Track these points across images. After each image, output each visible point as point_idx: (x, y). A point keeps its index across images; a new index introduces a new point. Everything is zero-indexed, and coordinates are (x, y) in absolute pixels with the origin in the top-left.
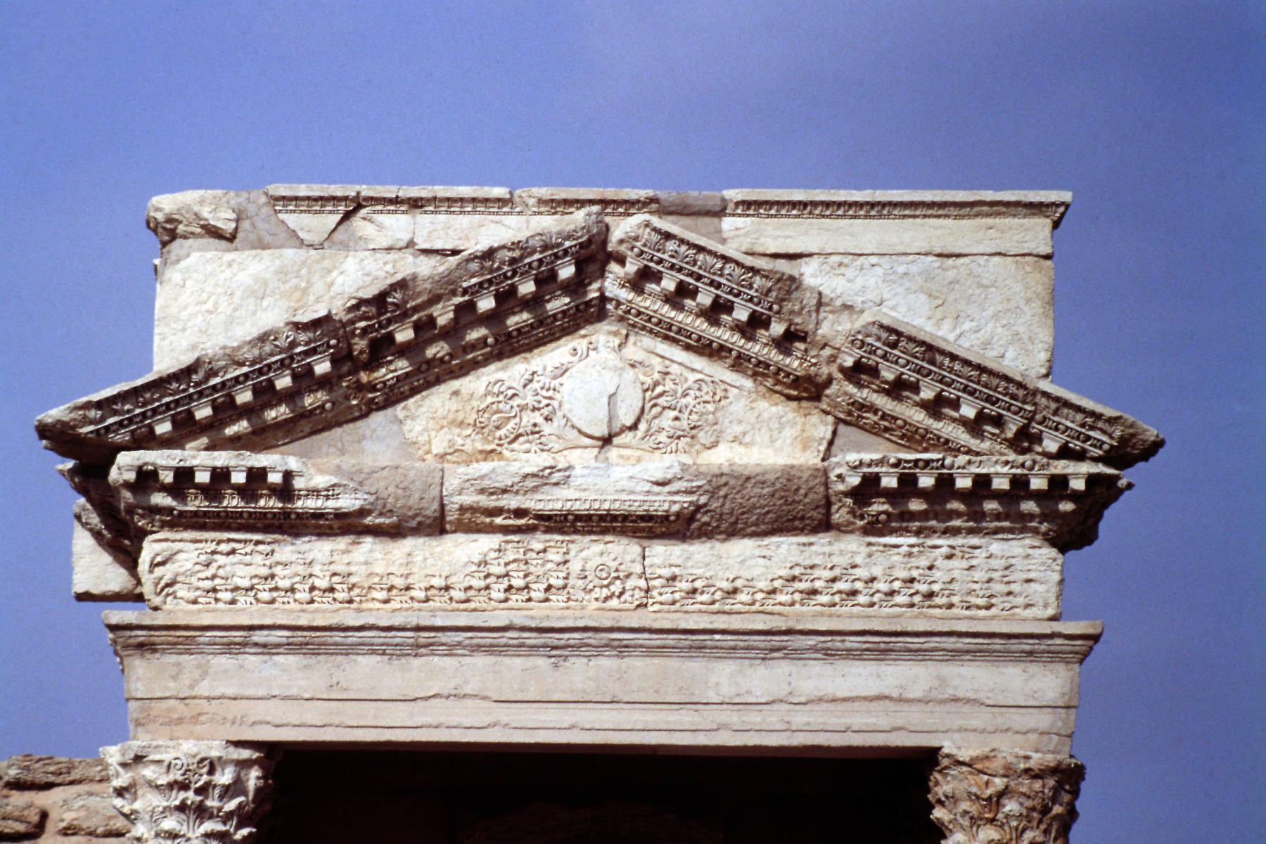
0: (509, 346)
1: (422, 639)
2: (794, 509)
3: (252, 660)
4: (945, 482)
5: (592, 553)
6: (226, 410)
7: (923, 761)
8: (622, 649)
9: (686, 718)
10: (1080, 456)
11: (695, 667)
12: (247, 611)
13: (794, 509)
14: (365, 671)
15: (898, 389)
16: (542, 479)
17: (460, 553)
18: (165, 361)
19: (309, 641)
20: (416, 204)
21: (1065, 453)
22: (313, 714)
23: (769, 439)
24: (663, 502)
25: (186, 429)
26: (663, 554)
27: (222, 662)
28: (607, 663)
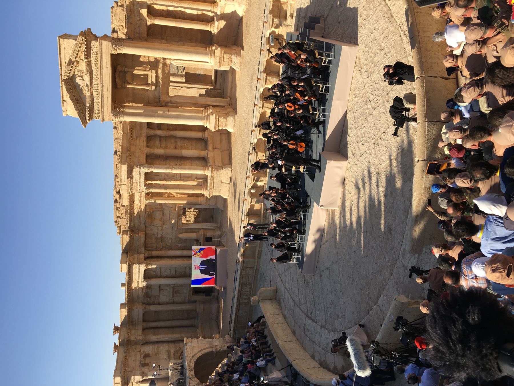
1: (102, 97)
2: (89, 64)
6: (83, 113)
7: (112, 55)
11: (104, 74)
12: (100, 111)
13: (89, 64)
14: (105, 102)
15: (77, 54)
18: (78, 117)
19: (103, 107)
20: (63, 95)
22: (109, 107)
23: (83, 66)
24: (89, 76)
25: (85, 116)
28: (104, 82)
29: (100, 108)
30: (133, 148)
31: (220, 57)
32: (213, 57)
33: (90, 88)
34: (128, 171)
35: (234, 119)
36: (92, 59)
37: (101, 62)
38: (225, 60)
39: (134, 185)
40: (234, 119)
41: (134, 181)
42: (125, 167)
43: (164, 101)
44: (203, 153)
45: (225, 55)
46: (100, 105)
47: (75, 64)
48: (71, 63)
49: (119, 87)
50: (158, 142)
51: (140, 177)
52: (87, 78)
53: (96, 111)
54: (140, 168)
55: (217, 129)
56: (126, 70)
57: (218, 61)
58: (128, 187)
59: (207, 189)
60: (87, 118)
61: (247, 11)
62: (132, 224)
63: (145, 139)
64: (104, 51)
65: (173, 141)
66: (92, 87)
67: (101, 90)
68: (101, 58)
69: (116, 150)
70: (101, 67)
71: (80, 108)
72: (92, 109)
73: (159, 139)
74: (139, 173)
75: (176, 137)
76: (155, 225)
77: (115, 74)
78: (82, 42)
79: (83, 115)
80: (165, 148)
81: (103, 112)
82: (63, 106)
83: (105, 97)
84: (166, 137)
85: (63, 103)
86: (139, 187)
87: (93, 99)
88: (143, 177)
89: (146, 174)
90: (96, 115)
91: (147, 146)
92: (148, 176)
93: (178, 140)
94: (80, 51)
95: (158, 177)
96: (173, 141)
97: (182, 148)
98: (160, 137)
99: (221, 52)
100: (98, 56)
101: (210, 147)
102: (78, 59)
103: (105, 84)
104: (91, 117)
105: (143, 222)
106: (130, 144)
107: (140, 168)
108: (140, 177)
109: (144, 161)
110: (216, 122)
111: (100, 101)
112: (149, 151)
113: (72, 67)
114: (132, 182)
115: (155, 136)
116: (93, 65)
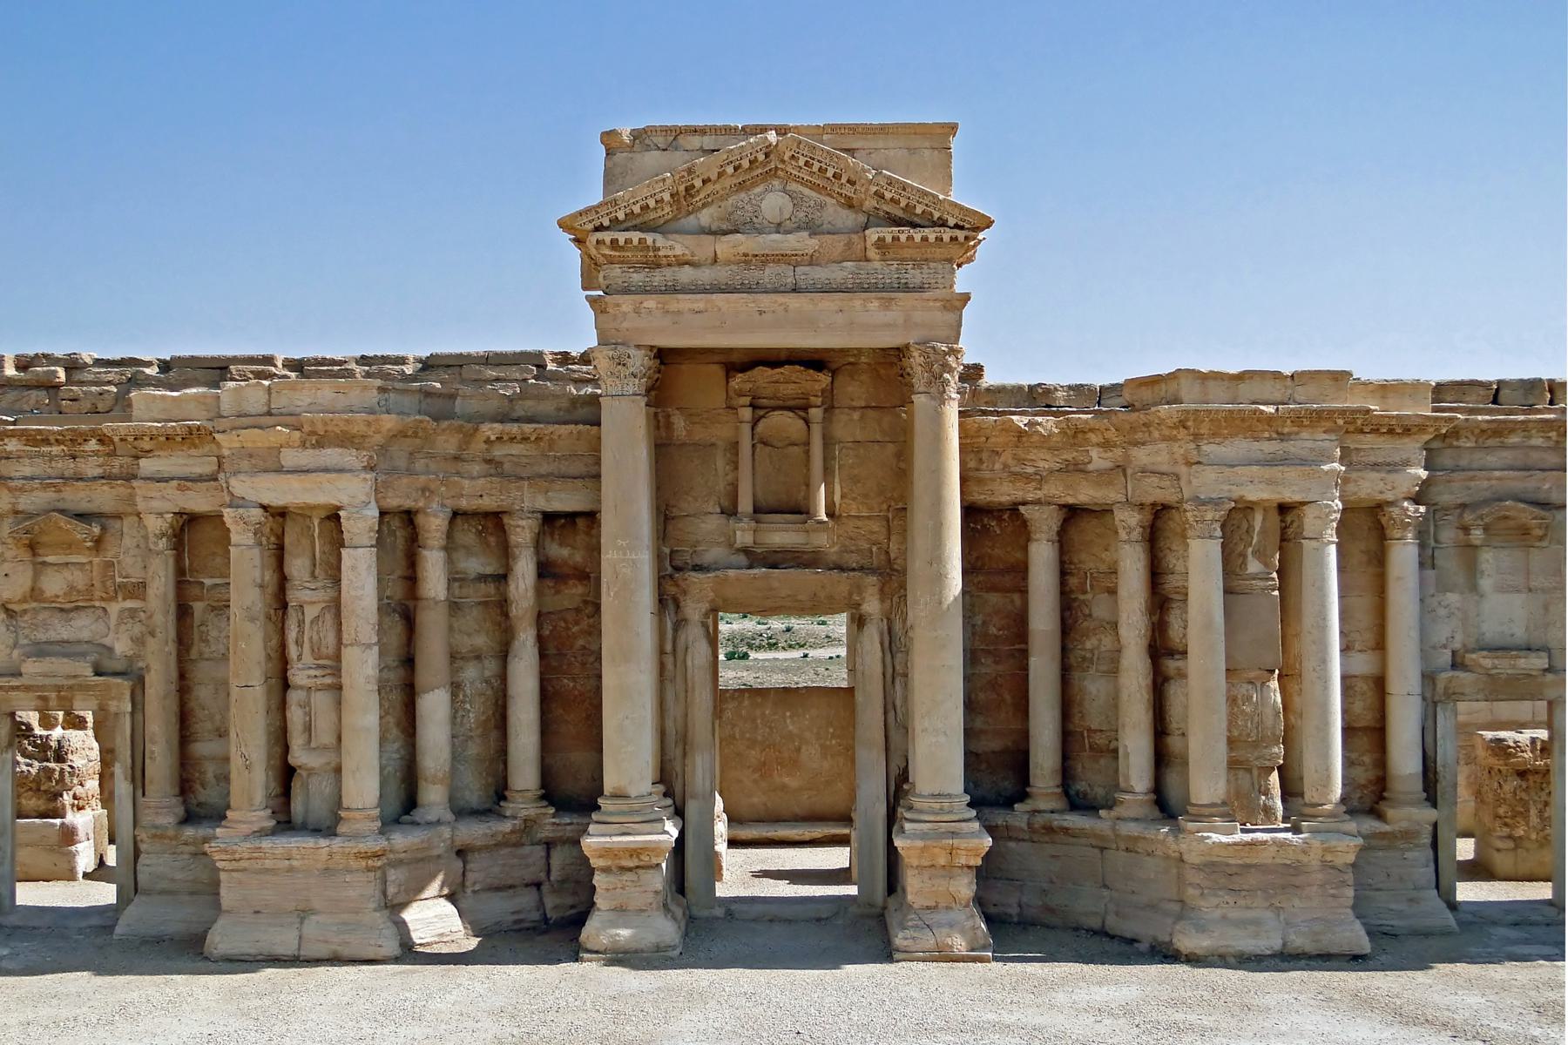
0: (741, 186)
4: (910, 238)
10: (962, 228)
21: (957, 226)
43: (685, 593)
44: (433, 796)
49: (738, 381)
50: (475, 565)
55: (594, 862)
56: (816, 414)
63: (488, 503)
65: (481, 641)
71: (652, 203)
73: (489, 570)
75: (504, 655)
77: (790, 362)
79: (621, 216)
80: (454, 607)
84: (502, 605)
91: (456, 514)
93: (491, 667)
96: (481, 641)
97: (456, 687)
98: (502, 578)
109: (393, 502)
112: (434, 525)
115: (505, 552)
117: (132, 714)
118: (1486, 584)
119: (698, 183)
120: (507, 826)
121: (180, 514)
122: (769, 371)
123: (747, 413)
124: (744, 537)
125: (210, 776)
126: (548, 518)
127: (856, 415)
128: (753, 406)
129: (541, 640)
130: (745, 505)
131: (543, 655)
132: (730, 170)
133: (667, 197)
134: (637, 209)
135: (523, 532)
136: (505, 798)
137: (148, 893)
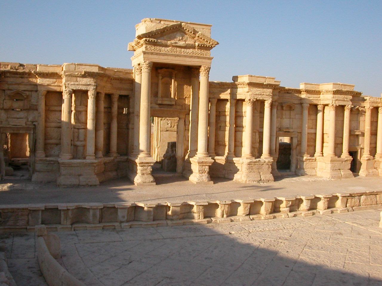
0: (173, 32)
3: (153, 55)
5: (178, 49)
8: (180, 57)
9: (184, 62)
12: (153, 51)
13: (193, 47)
14: (161, 57)
15: (201, 38)
16: (176, 43)
17: (169, 48)
19: (157, 54)
23: (190, 42)
24: (183, 45)
25: (149, 37)
26: (183, 50)
27: (151, 55)
28: (179, 57)
29: (156, 51)
30: (105, 79)
31: (206, 163)
32: (205, 156)
33: (174, 45)
34: (90, 72)
35: (152, 182)
36: (196, 50)
37: (195, 57)
38: (204, 167)
39: (75, 79)
40: (152, 182)
41: (78, 79)
42: (95, 70)
45: (207, 167)
46: (158, 52)
47: (193, 35)
48: (195, 32)
49: (159, 71)
51: (84, 85)
52: (182, 43)
53: (153, 48)
54: (94, 86)
57: (203, 160)
58: (72, 72)
59: (70, 159)
60: (148, 39)
61: (237, 183)
62: (8, 75)
63: (111, 92)
64: (204, 60)
66: (173, 46)
67: (169, 55)
68: (199, 57)
69: (24, 66)
70: (192, 57)
72: (155, 44)
74: (88, 85)
76: (5, 101)
78: (211, 44)
79: (150, 35)
81: (152, 54)
82: (156, 20)
83: (166, 57)
85: (158, 20)
86: (72, 83)
87: (163, 47)
88: (84, 88)
89: (86, 92)
90: (148, 47)
92: (81, 95)
94: (203, 41)
95: (79, 104)
99: (210, 163)
100: (199, 55)
101: (107, 159)
102: (196, 38)
103: (177, 58)
104: (148, 43)
105: (11, 87)
106: (109, 77)
107: (94, 86)
108: (84, 85)
110: (147, 163)
111: (162, 52)
113: (191, 32)
114: (78, 77)
116: (191, 50)
117: (33, 134)
118: (284, 117)
119: (166, 31)
120: (112, 158)
121: (47, 91)
122: (165, 69)
123: (161, 77)
124: (159, 102)
125: (49, 147)
126: (121, 97)
127: (180, 80)
128: (162, 77)
129: (117, 121)
130: (160, 95)
131: (118, 124)
132: (172, 29)
133: (159, 33)
134: (154, 34)
135: (115, 99)
136: (109, 153)
137: (37, 171)
